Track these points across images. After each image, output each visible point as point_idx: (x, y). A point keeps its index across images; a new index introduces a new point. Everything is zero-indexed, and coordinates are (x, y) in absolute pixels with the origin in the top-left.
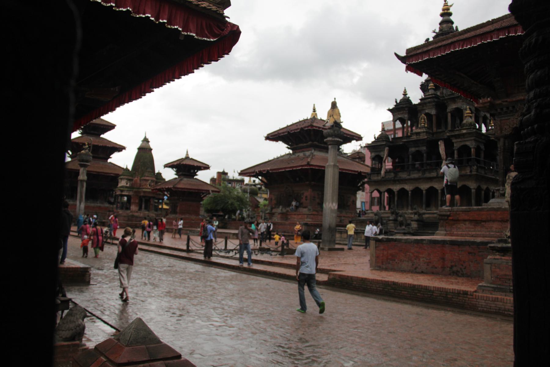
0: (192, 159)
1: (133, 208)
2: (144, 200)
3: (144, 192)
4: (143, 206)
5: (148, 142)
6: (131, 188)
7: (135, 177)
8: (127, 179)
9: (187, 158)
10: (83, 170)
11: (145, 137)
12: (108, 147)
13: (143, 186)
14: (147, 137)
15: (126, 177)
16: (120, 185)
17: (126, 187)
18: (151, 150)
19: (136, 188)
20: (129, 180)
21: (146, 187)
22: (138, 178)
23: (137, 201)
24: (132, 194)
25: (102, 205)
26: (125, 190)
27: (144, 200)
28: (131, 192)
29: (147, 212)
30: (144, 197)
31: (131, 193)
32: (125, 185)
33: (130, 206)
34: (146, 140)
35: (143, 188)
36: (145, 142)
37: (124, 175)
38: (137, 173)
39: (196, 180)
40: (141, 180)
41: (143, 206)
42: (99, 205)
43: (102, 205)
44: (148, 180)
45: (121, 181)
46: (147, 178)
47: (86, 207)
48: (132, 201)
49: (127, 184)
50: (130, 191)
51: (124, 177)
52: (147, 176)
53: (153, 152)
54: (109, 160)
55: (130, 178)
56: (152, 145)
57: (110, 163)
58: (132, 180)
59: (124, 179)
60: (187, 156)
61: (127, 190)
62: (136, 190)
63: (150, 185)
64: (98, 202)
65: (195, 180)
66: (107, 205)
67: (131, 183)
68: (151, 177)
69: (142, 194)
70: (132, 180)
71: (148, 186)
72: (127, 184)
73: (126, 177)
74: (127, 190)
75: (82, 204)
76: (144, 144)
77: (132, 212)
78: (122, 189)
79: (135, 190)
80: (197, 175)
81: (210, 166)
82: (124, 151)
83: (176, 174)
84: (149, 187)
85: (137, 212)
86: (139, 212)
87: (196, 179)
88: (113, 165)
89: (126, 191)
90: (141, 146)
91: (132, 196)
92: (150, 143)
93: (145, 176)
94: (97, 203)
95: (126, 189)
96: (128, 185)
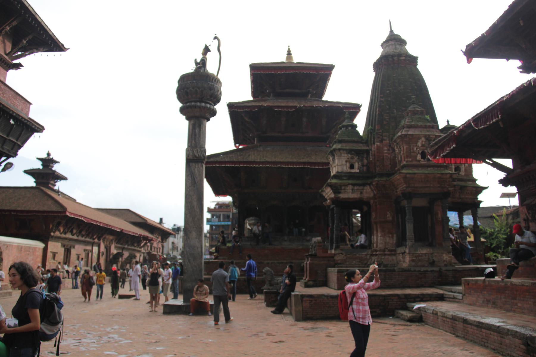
4: (409, 228)
5: (403, 42)
7: (374, 143)
8: (350, 151)
11: (391, 31)
14: (396, 32)
15: (348, 146)
16: (334, 172)
17: (351, 176)
18: (413, 60)
19: (381, 175)
20: (358, 153)
21: (414, 163)
22: (381, 141)
23: (389, 217)
28: (368, 189)
29: (425, 251)
31: (368, 192)
32: (346, 169)
36: (390, 43)
41: (409, 228)
49: (352, 167)
50: (364, 185)
52: (410, 127)
53: (421, 67)
56: (411, 49)
63: (423, 155)
67: (365, 161)
68: (426, 127)
70: (367, 152)
71: (419, 157)
72: (352, 167)
73: (348, 146)
74: (354, 185)
76: (391, 50)
84: (423, 162)
89: (350, 187)
91: (372, 202)
92: (407, 47)
93: (403, 127)
95: (350, 182)
96: (356, 170)
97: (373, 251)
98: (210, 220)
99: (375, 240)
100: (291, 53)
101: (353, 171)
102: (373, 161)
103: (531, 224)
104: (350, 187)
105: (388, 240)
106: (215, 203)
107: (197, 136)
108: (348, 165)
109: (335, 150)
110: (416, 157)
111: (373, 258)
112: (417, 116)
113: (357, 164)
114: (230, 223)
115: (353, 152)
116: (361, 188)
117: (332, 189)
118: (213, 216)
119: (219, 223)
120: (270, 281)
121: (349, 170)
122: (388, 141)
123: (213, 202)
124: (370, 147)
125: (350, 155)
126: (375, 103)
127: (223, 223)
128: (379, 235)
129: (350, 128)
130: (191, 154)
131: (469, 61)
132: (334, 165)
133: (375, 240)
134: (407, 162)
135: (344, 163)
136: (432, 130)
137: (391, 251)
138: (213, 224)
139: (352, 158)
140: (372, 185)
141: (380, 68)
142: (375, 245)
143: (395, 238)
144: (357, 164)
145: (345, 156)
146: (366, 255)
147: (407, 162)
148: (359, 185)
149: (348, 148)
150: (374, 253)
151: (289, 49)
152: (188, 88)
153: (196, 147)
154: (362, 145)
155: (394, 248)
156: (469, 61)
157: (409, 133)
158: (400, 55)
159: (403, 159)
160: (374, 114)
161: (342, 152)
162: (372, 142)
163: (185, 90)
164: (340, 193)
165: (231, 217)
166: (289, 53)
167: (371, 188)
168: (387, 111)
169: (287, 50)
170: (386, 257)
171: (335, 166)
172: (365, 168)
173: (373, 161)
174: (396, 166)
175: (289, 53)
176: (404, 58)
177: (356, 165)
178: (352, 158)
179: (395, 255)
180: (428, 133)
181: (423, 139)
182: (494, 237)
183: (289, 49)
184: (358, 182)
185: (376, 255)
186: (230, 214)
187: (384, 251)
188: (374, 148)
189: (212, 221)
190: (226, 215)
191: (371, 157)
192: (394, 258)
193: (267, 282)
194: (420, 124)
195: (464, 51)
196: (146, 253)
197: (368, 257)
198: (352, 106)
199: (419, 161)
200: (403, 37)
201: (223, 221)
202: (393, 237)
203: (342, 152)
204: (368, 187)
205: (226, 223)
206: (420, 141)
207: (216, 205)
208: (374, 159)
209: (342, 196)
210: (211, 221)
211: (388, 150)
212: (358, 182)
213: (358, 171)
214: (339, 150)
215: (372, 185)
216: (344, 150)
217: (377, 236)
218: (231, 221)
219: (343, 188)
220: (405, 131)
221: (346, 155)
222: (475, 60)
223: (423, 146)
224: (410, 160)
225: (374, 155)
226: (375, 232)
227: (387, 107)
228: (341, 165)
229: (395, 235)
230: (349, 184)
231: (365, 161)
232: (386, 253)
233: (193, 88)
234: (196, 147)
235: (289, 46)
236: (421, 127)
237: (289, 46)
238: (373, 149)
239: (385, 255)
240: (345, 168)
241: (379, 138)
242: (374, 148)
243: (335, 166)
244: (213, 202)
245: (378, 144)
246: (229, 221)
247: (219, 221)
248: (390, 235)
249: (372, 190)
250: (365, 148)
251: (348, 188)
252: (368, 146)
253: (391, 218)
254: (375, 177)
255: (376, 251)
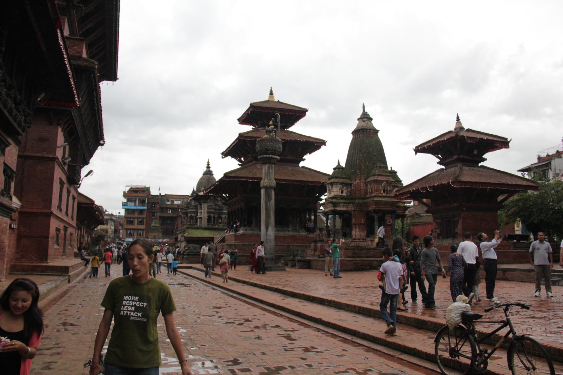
0: (469, 130)
1: (357, 233)
2: (376, 217)
3: (377, 203)
6: (349, 199)
7: (355, 180)
9: (460, 128)
10: (269, 169)
11: (364, 111)
12: (300, 142)
13: (371, 193)
15: (341, 180)
17: (342, 198)
19: (359, 199)
20: (346, 185)
21: (380, 195)
22: (360, 180)
23: (363, 221)
24: (353, 209)
25: (296, 234)
26: (340, 203)
27: (376, 217)
28: (351, 205)
30: (375, 211)
31: (351, 208)
32: (339, 193)
33: (351, 230)
34: (365, 117)
35: (374, 197)
37: (337, 178)
38: (358, 171)
39: (483, 169)
40: (366, 184)
42: (291, 233)
43: (296, 234)
44: (381, 182)
45: (332, 187)
46: (380, 178)
47: (276, 237)
48: (353, 220)
49: (342, 192)
50: (349, 203)
51: (336, 180)
52: (379, 175)
53: (380, 135)
54: (302, 164)
55: (347, 181)
56: (376, 124)
57: (303, 167)
58: (351, 184)
59: (337, 183)
60: (459, 126)
61: (344, 203)
62: (361, 201)
63: (384, 191)
64: (290, 229)
65: (480, 169)
66: (304, 233)
67: (349, 189)
68: (386, 176)
69: (371, 208)
70: (351, 184)
71: (382, 192)
72: (342, 192)
73: (341, 180)
75: (270, 229)
77: (354, 240)
78: (335, 200)
79: (357, 201)
80: (484, 160)
81: (509, 140)
82: (323, 147)
83: (439, 163)
84: (384, 194)
85: (364, 240)
86: (368, 239)
87: (482, 166)
88: (308, 170)
89: (342, 204)
90: (358, 127)
91: (352, 212)
93: (375, 175)
94: (289, 231)
95: (342, 201)
96: (344, 194)
97: (353, 239)
98: (125, 204)
99: (354, 233)
100: (273, 93)
101: (343, 195)
102: (354, 190)
103: (437, 230)
104: (342, 204)
105: (362, 234)
106: (129, 188)
107: (271, 174)
108: (341, 191)
109: (334, 183)
110: (381, 191)
111: (354, 243)
112: (381, 169)
113: (345, 191)
114: (145, 208)
115: (344, 184)
116: (348, 205)
117: (333, 205)
118: (129, 200)
119: (135, 208)
120: (300, 255)
121: (341, 194)
122: (363, 180)
123: (127, 186)
124: (352, 181)
125: (342, 186)
126: (355, 156)
127: (139, 208)
128: (357, 230)
129: (341, 169)
130: (268, 184)
131: (416, 154)
132: (332, 190)
133: (354, 233)
134: (376, 194)
135: (338, 190)
136: (389, 177)
137: (363, 239)
138: (129, 208)
139: (343, 187)
140: (355, 204)
141: (358, 135)
142: (354, 236)
143: (365, 233)
144: (345, 191)
145: (339, 186)
146: (349, 241)
147: (376, 194)
148: (347, 203)
149: (341, 181)
150: (354, 240)
151: (271, 90)
152: (268, 147)
153: (270, 180)
154: (347, 180)
155: (365, 238)
156: (416, 154)
157: (379, 179)
158: (370, 129)
159: (374, 192)
160: (355, 164)
161: (338, 184)
162: (354, 179)
163: (266, 148)
164: (336, 207)
165: (146, 202)
166: (271, 93)
167: (353, 205)
168: (363, 163)
169: (269, 90)
170: (361, 243)
171: (333, 191)
172: (349, 193)
173: (354, 190)
174: (367, 194)
175: (271, 93)
176: (372, 131)
177: (345, 192)
178: (343, 187)
179: (365, 241)
180: (388, 180)
181: (385, 182)
182: (398, 232)
183: (271, 90)
184: (346, 201)
185: (355, 241)
186: (145, 199)
187: (359, 239)
188: (355, 183)
189: (128, 205)
190: (142, 200)
191: (352, 187)
192: (365, 243)
193: (299, 255)
194: (383, 174)
195: (414, 148)
196: (105, 236)
197: (350, 242)
198: (321, 141)
199: (382, 194)
200: (371, 116)
201: (138, 206)
202: (364, 232)
203: (338, 184)
204: (352, 204)
205: (142, 208)
206: (383, 183)
207: (131, 188)
208: (355, 189)
209: (338, 209)
210: (126, 205)
211: (363, 185)
212: (346, 201)
213: (345, 195)
214: (337, 183)
215: (355, 204)
216: (339, 183)
217: (356, 231)
218: (146, 205)
219: (339, 204)
220: (377, 178)
221: (340, 186)
222: (418, 154)
223: (384, 186)
224: (378, 193)
225: (355, 187)
226: (354, 229)
227: (363, 160)
228: (337, 191)
229: (365, 231)
230: (342, 202)
231: (349, 189)
232: (361, 240)
233: (271, 147)
234: (270, 180)
235: (271, 88)
236: (384, 175)
237: (271, 88)
238: (354, 183)
239: (360, 241)
240: (339, 193)
241: (358, 178)
242: (355, 183)
243: (333, 191)
244: (127, 186)
245: (358, 181)
246: (145, 206)
247: (135, 205)
248: (363, 231)
249: (354, 206)
250: (350, 182)
251: (341, 205)
252: (351, 181)
253: (364, 222)
254: (356, 199)
255: (355, 239)
